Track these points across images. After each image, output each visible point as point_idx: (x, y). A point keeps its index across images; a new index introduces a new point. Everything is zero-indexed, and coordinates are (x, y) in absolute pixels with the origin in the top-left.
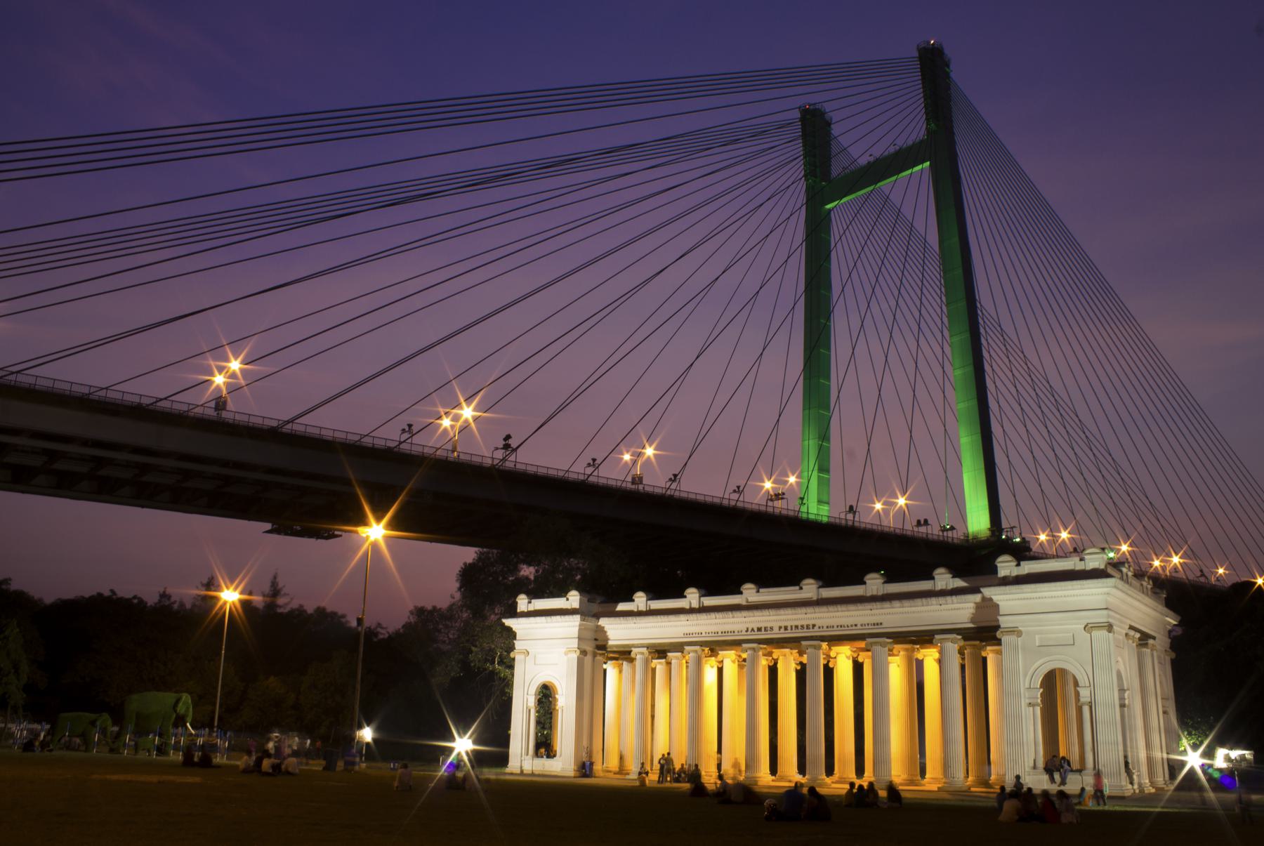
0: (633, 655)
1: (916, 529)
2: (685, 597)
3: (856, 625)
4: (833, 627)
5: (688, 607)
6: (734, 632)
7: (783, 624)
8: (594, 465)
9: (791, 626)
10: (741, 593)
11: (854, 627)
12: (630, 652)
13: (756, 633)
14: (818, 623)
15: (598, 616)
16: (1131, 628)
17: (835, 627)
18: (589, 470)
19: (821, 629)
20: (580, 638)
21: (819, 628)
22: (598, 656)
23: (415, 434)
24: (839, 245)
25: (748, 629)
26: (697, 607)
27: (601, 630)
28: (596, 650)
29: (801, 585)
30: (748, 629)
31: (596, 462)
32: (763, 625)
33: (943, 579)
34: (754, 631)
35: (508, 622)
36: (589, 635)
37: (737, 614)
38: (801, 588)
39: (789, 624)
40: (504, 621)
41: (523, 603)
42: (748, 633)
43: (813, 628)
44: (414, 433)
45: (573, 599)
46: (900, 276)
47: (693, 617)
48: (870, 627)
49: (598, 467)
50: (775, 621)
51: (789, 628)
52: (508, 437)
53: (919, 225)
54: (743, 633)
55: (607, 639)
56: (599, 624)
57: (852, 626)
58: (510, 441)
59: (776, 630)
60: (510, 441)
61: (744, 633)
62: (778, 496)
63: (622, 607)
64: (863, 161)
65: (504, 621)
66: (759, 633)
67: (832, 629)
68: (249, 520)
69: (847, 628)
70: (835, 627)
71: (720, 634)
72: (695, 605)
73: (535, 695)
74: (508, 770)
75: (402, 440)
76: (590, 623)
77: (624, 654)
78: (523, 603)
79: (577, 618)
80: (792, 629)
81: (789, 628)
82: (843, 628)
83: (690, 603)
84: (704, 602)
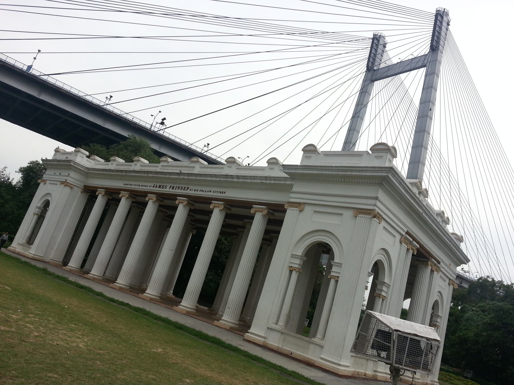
16: (407, 233)
17: (199, 191)
18: (206, 149)
24: (374, 99)
34: (157, 188)
46: (401, 124)
52: (164, 119)
53: (411, 92)
58: (164, 121)
59: (168, 187)
60: (164, 121)
64: (395, 61)
66: (159, 189)
68: (43, 135)
70: (199, 191)
80: (176, 189)
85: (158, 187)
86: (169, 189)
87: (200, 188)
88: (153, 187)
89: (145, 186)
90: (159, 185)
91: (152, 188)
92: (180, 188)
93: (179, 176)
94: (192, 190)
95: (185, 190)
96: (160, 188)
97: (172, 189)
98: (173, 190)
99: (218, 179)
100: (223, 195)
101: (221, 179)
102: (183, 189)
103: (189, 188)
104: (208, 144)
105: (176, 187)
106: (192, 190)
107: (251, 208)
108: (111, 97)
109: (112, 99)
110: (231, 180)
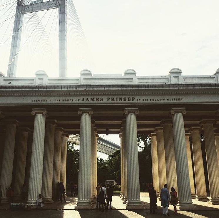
13: (90, 102)
21: (137, 100)
34: (88, 101)
43: (133, 100)
66: (92, 102)
70: (149, 100)
80: (117, 101)
81: (115, 99)
85: (90, 100)
86: (108, 101)
87: (149, 98)
88: (83, 100)
89: (68, 100)
90: (91, 98)
91: (81, 102)
92: (123, 99)
93: (104, 88)
94: (140, 99)
95: (130, 101)
96: (94, 101)
97: (112, 101)
98: (113, 102)
99: (177, 88)
100: (181, 101)
101: (180, 88)
103: (134, 98)
105: (117, 98)
106: (140, 99)
107: (123, 110)
110: (192, 88)
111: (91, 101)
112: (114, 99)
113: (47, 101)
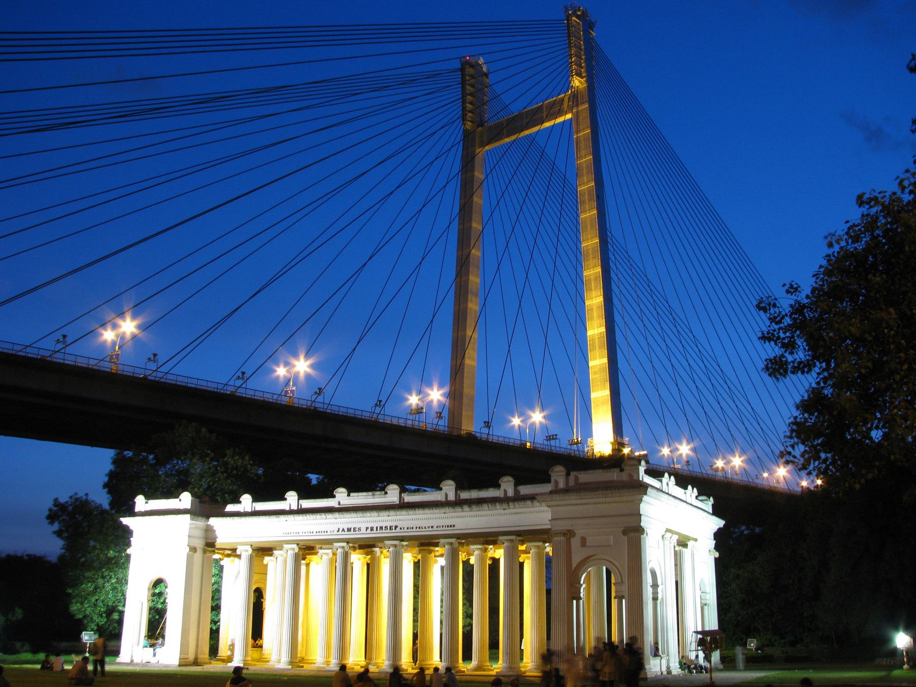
0: (238, 552)
1: (546, 442)
2: (286, 499)
3: (432, 527)
4: (413, 528)
5: (288, 509)
6: (327, 532)
7: (369, 525)
8: (243, 378)
9: (377, 528)
10: (334, 497)
11: (430, 529)
12: (234, 550)
14: (399, 524)
15: (208, 517)
16: (668, 530)
17: (415, 528)
18: (239, 383)
19: (402, 530)
20: (189, 536)
21: (401, 529)
22: (208, 552)
23: (68, 345)
25: (339, 529)
26: (296, 509)
27: (209, 530)
28: (206, 547)
29: (386, 490)
30: (339, 529)
31: (245, 375)
32: (352, 526)
33: (507, 486)
34: (344, 531)
35: (125, 521)
36: (199, 533)
37: (329, 516)
38: (386, 493)
39: (375, 525)
40: (122, 519)
41: (141, 503)
42: (340, 533)
43: (395, 529)
44: (67, 344)
45: (186, 500)
47: (291, 518)
48: (444, 528)
49: (246, 381)
50: (364, 525)
51: (375, 529)
54: (334, 533)
55: (215, 538)
56: (209, 523)
57: (429, 527)
59: (363, 530)
61: (336, 533)
62: (419, 411)
63: (230, 508)
65: (122, 519)
66: (349, 533)
67: (411, 530)
69: (424, 530)
70: (415, 528)
71: (315, 533)
72: (294, 507)
73: (149, 589)
74: (119, 660)
75: (57, 350)
76: (200, 523)
77: (233, 552)
78: (141, 503)
79: (188, 516)
80: (377, 530)
81: (375, 529)
82: (421, 530)
83: (290, 505)
84: (303, 504)
86: (366, 530)
90: (348, 528)
95: (392, 529)
102: (389, 529)
104: (243, 373)
108: (65, 336)
109: (67, 339)
111: (347, 531)
112: (373, 528)
113: (299, 533)
